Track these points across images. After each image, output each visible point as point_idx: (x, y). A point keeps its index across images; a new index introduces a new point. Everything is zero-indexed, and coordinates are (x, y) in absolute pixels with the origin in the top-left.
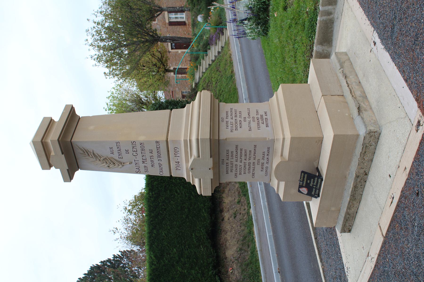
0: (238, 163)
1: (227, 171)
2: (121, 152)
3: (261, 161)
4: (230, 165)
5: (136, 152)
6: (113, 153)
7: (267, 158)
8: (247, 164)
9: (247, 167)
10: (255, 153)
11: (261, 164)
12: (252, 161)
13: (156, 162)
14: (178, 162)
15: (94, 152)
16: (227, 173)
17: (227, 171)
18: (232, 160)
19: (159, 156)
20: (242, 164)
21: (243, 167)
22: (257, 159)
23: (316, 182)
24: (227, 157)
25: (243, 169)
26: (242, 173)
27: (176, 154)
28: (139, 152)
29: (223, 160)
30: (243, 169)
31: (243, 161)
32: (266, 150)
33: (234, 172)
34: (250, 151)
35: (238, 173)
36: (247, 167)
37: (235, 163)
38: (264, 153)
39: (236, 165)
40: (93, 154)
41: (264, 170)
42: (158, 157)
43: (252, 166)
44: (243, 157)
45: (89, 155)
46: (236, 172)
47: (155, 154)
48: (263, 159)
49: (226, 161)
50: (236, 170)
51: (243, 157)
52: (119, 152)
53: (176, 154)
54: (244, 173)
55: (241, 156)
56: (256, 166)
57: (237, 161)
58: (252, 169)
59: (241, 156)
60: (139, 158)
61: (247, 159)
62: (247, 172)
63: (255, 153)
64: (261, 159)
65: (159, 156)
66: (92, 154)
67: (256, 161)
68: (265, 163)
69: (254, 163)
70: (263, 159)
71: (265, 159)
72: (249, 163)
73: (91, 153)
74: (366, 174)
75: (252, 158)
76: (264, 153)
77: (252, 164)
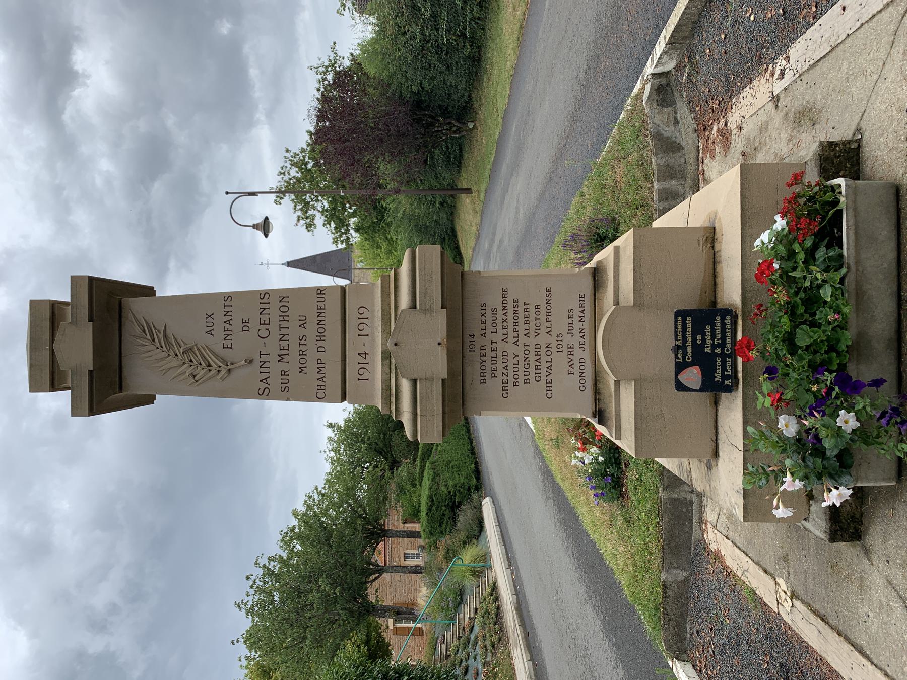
0: (511, 349)
2: (230, 328)
3: (567, 340)
5: (267, 327)
9: (532, 358)
12: (543, 339)
13: (312, 355)
14: (365, 354)
15: (168, 331)
18: (494, 337)
19: (320, 337)
20: (520, 350)
21: (521, 358)
24: (483, 326)
27: (361, 327)
28: (274, 327)
31: (523, 340)
36: (532, 358)
37: (501, 346)
38: (571, 314)
39: (505, 354)
40: (165, 336)
41: (576, 370)
43: (544, 358)
44: (521, 327)
45: (154, 340)
46: (505, 378)
47: (311, 330)
48: (570, 332)
50: (505, 371)
52: (227, 326)
53: (361, 327)
56: (555, 356)
58: (544, 366)
60: (273, 346)
61: (532, 334)
63: (549, 314)
64: (565, 331)
66: (161, 336)
68: (577, 346)
70: (570, 332)
71: (576, 332)
72: (537, 346)
73: (160, 333)
75: (543, 330)
76: (571, 314)
77: (543, 349)
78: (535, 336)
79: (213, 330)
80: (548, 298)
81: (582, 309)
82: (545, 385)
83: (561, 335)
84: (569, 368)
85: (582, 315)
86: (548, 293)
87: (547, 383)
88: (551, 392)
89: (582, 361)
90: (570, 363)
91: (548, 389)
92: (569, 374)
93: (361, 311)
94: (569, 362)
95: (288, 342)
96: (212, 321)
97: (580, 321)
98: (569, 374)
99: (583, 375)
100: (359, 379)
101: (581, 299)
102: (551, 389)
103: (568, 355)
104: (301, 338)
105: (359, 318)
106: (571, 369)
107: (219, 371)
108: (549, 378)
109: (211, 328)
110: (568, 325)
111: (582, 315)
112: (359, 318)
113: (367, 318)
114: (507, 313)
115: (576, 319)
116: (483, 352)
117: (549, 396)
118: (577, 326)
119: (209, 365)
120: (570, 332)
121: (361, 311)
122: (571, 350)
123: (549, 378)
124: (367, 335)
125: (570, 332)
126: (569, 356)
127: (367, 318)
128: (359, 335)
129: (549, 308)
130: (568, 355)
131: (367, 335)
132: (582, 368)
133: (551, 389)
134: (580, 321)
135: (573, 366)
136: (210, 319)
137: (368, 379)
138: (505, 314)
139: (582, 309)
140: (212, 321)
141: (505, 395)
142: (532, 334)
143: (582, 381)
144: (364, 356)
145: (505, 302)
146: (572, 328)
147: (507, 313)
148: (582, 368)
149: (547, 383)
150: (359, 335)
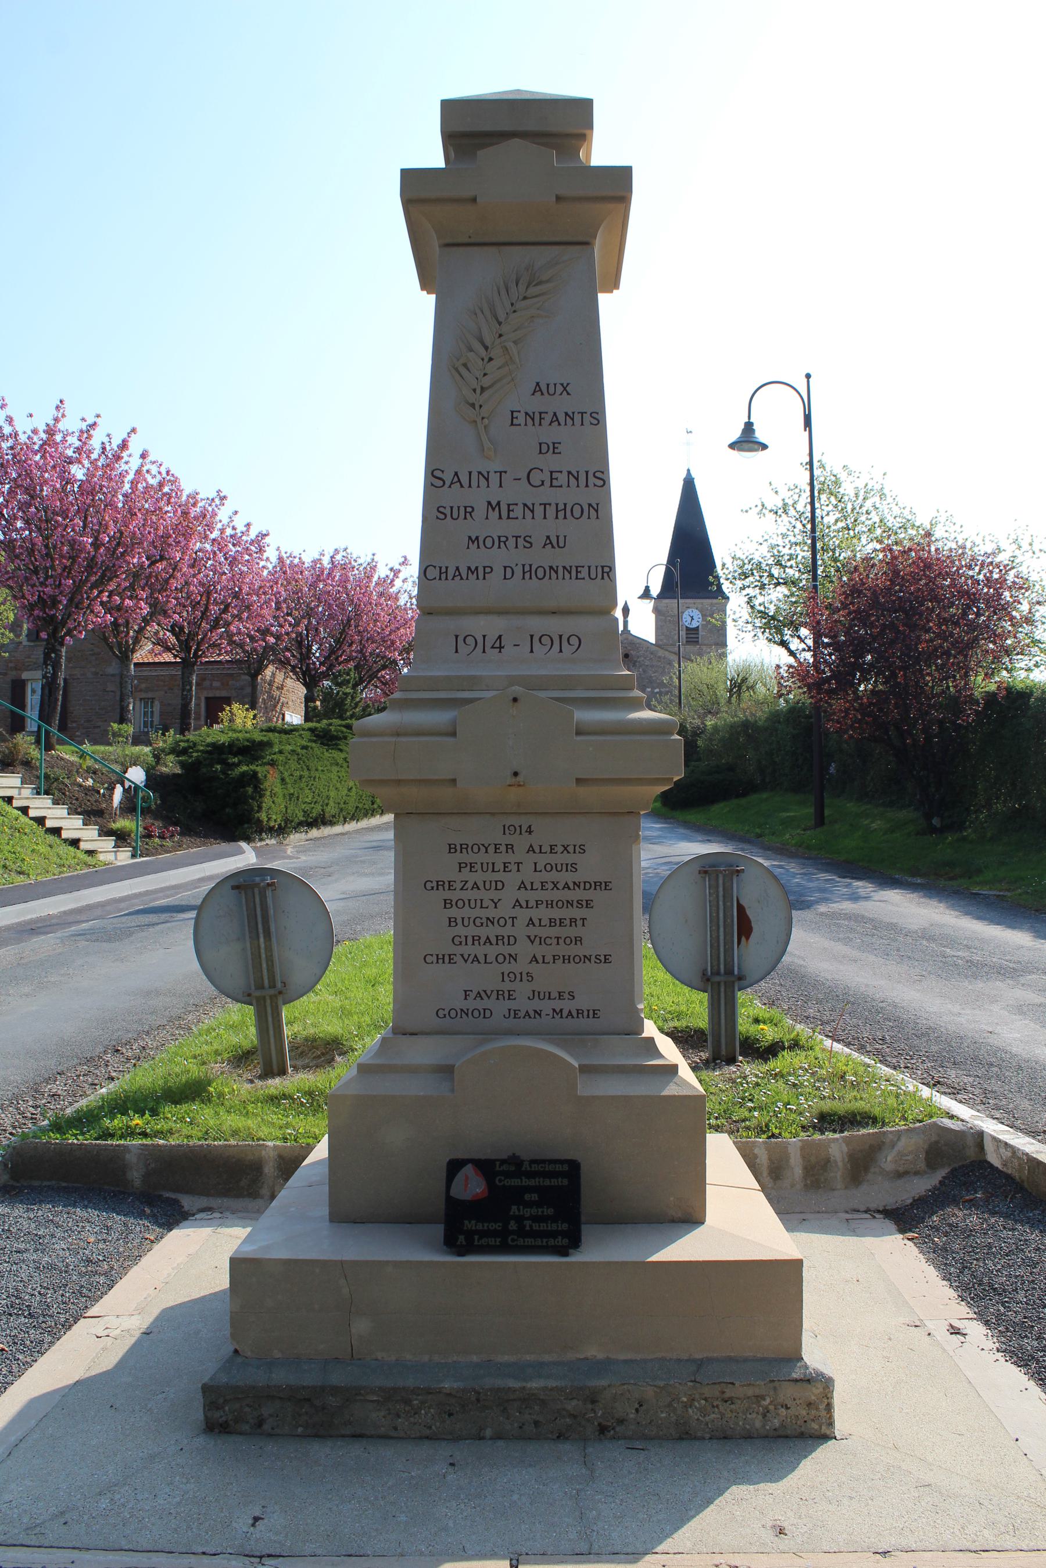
0: (509, 895)
1: (464, 847)
2: (544, 422)
3: (523, 989)
4: (499, 860)
5: (547, 483)
6: (538, 389)
7: (538, 1013)
8: (506, 931)
9: (492, 931)
10: (567, 959)
11: (507, 986)
13: (498, 557)
14: (501, 647)
16: (452, 848)
17: (464, 847)
18: (527, 868)
19: (529, 572)
20: (505, 910)
21: (491, 913)
22: (534, 968)
23: (553, 1227)
24: (546, 848)
25: (478, 912)
26: (454, 912)
27: (546, 640)
28: (547, 494)
29: (530, 832)
30: (478, 912)
31: (523, 915)
32: (583, 1002)
33: (458, 877)
34: (578, 940)
35: (454, 896)
36: (492, 931)
37: (512, 879)
38: (566, 996)
41: (471, 1004)
42: (527, 568)
43: (492, 951)
44: (544, 913)
46: (459, 885)
48: (535, 995)
49: (521, 842)
50: (469, 885)
51: (544, 913)
52: (548, 418)
53: (546, 640)
54: (452, 922)
55: (550, 904)
57: (522, 886)
58: (479, 950)
59: (550, 904)
60: (515, 492)
61: (533, 931)
62: (460, 930)
63: (567, 959)
65: (529, 572)
67: (522, 966)
68: (513, 1005)
69: (513, 958)
70: (535, 995)
71: (536, 1005)
72: (511, 940)
74: (603, 1430)
75: (539, 950)
76: (566, 996)
77: (507, 950)
78: (529, 937)
79: (542, 394)
80: (593, 959)
81: (575, 1014)
82: (447, 952)
83: (530, 979)
85: (565, 1013)
87: (450, 955)
90: (483, 994)
91: (440, 956)
92: (465, 991)
93: (574, 641)
94: (485, 991)
95: (521, 516)
96: (559, 391)
97: (554, 1010)
98: (465, 991)
100: (457, 637)
101: (591, 1013)
102: (441, 961)
103: (498, 991)
104: (527, 539)
105: (561, 636)
106: (473, 995)
107: (473, 405)
109: (545, 390)
111: (565, 1013)
112: (561, 636)
113: (561, 651)
115: (558, 1005)
116: (503, 848)
117: (429, 959)
118: (546, 1006)
119: (483, 389)
120: (536, 994)
121: (574, 641)
122: (506, 995)
124: (532, 651)
125: (536, 994)
126: (495, 993)
127: (561, 651)
128: (532, 636)
129: (577, 959)
130: (498, 991)
131: (532, 651)
132: (476, 1013)
133: (441, 961)
134: (554, 1010)
135: (478, 999)
136: (560, 389)
137: (457, 651)
138: (566, 886)
139: (575, 1014)
140: (559, 391)
142: (533, 931)
144: (497, 645)
148: (476, 1013)
149: (450, 955)
150: (532, 636)
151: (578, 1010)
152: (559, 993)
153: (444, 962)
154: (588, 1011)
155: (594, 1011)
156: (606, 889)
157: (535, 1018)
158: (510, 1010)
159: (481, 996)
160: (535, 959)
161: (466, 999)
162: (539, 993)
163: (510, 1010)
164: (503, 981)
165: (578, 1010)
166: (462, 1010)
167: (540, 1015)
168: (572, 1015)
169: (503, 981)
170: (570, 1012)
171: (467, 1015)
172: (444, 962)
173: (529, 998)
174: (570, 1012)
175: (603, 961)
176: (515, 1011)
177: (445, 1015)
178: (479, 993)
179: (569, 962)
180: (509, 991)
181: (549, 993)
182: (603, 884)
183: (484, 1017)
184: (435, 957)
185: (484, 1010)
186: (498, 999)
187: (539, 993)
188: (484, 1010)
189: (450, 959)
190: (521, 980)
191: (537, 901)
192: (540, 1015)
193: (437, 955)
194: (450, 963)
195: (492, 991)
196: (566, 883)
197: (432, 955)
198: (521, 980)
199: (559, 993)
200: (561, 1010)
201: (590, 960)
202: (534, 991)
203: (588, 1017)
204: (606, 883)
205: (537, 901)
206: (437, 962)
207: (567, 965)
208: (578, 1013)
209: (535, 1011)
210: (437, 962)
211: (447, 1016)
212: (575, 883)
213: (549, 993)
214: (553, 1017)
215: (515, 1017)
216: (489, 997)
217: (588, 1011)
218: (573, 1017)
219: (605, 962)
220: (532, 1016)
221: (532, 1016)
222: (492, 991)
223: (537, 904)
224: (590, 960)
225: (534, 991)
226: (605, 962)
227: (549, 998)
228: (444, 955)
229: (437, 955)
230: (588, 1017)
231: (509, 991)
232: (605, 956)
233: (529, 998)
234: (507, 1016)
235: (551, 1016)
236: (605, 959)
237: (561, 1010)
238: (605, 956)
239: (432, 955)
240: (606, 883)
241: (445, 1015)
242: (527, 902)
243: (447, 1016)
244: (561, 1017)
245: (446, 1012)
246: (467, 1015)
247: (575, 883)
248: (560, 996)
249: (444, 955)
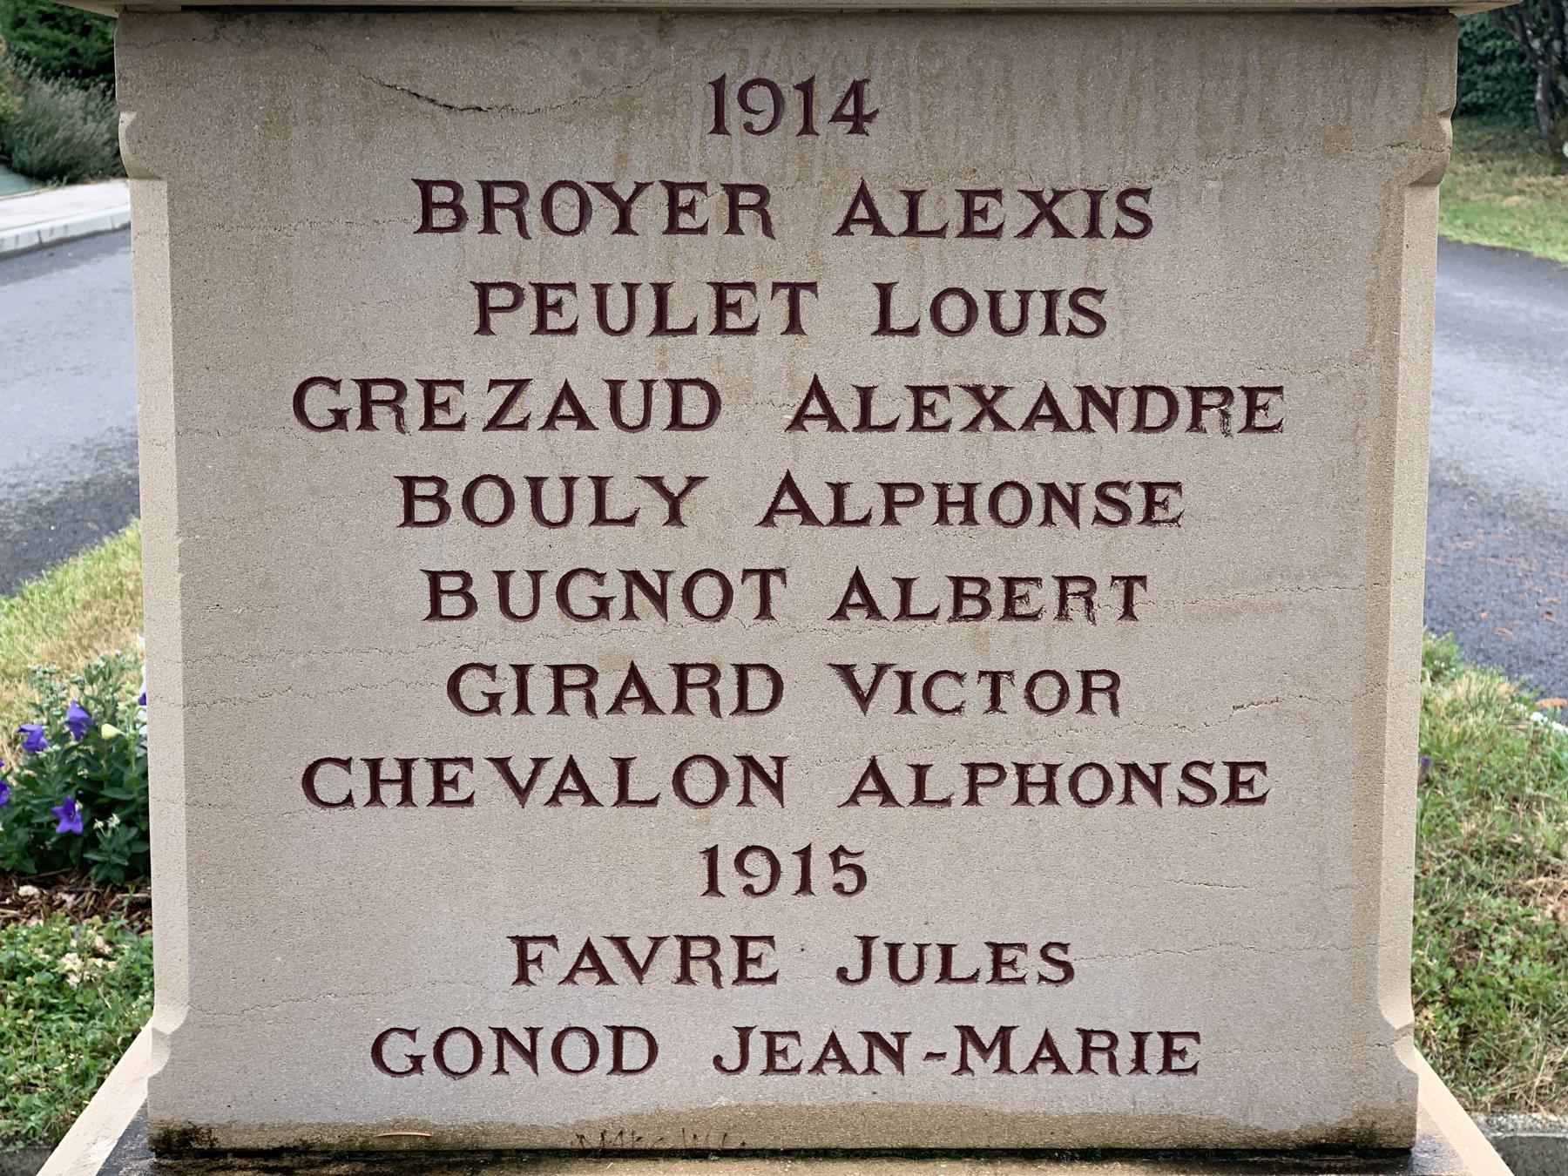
38: (1030, 964)
46: (478, 404)
50: (537, 402)
76: (1030, 964)
78: (846, 672)
80: (1172, 782)
81: (1070, 1051)
82: (422, 748)
83: (849, 880)
84: (570, 950)
85: (1022, 1049)
86: (1220, 780)
87: (438, 765)
88: (363, 794)
89: (635, 1049)
90: (610, 956)
91: (390, 770)
92: (522, 942)
94: (621, 942)
97: (968, 1033)
98: (522, 942)
99: (512, 1058)
101: (1154, 1047)
102: (391, 794)
103: (685, 942)
106: (558, 961)
108: (481, 781)
110: (933, 938)
111: (1022, 1049)
114: (1060, 423)
117: (330, 783)
120: (880, 954)
122: (728, 960)
123: (481, 781)
125: (880, 954)
126: (672, 949)
129: (1091, 785)
130: (685, 942)
132: (575, 1052)
133: (391, 794)
134: (968, 1033)
135: (587, 980)
138: (1047, 410)
139: (1070, 1051)
141: (319, 404)
143: (458, 1052)
145: (1157, 409)
146: (907, 968)
147: (1060, 423)
148: (575, 1052)
149: (438, 765)
151: (1086, 1035)
152: (997, 949)
153: (407, 798)
154: (1140, 1038)
155: (1168, 1037)
156: (1249, 427)
157: (871, 1068)
158: (744, 1033)
159: (599, 967)
160: (875, 783)
161: (523, 977)
162: (894, 949)
163: (744, 1033)
164: (713, 888)
165: (1086, 1035)
166: (503, 1034)
167: (896, 1057)
168: (1055, 1057)
169: (713, 888)
170: (1047, 1041)
171: (530, 1056)
172: (407, 798)
173: (842, 973)
174: (1047, 1041)
175: (1223, 791)
176: (771, 1037)
177: (417, 1061)
178: (589, 949)
179: (1051, 798)
180: (742, 942)
181: (946, 950)
182: (1240, 400)
183: (617, 1067)
184: (362, 772)
185: (618, 1032)
186: (685, 977)
187: (894, 949)
188: (618, 1032)
189: (439, 782)
190: (805, 887)
191: (889, 489)
192: (896, 1057)
193: (374, 765)
194: (438, 799)
195: (657, 942)
196: (1046, 395)
197: (346, 764)
198: (805, 887)
199: (997, 949)
200: (1004, 1034)
201: (1155, 789)
202: (867, 942)
203: (1139, 1064)
204: (1251, 393)
205: (889, 489)
206: (375, 798)
207: (1038, 811)
208: (1087, 1050)
209: (874, 1038)
210: (375, 798)
211: (429, 1063)
212: (1088, 393)
213: (946, 950)
214: (964, 1067)
215: (771, 1068)
216: (639, 971)
217: (1140, 1038)
218: (1061, 1067)
219: (1233, 797)
220: (859, 1063)
221: (859, 1063)
222: (657, 942)
223: (891, 504)
224: (1155, 789)
225: (867, 942)
226: (1233, 797)
227: (945, 974)
228: (406, 765)
229: (374, 765)
230: (1139, 1064)
231: (742, 942)
232: (1234, 768)
233: (842, 973)
234: (732, 1061)
235: (953, 1061)
236: (1235, 784)
237: (1004, 1034)
238: (1234, 768)
239: (346, 764)
240: (1251, 393)
241: (417, 1061)
242: (839, 490)
243: (429, 1063)
244: (1005, 1065)
245: (425, 1046)
246: (530, 1056)
247: (1088, 393)
248: (997, 963)
249: (406, 765)
